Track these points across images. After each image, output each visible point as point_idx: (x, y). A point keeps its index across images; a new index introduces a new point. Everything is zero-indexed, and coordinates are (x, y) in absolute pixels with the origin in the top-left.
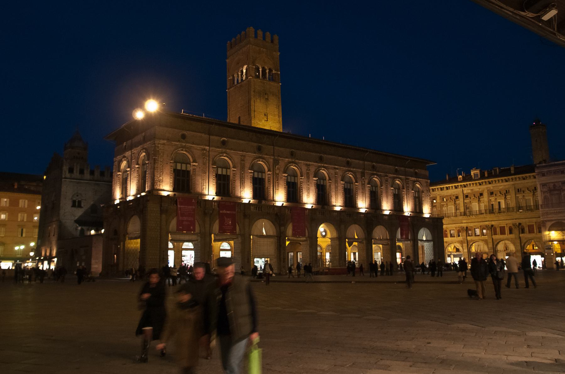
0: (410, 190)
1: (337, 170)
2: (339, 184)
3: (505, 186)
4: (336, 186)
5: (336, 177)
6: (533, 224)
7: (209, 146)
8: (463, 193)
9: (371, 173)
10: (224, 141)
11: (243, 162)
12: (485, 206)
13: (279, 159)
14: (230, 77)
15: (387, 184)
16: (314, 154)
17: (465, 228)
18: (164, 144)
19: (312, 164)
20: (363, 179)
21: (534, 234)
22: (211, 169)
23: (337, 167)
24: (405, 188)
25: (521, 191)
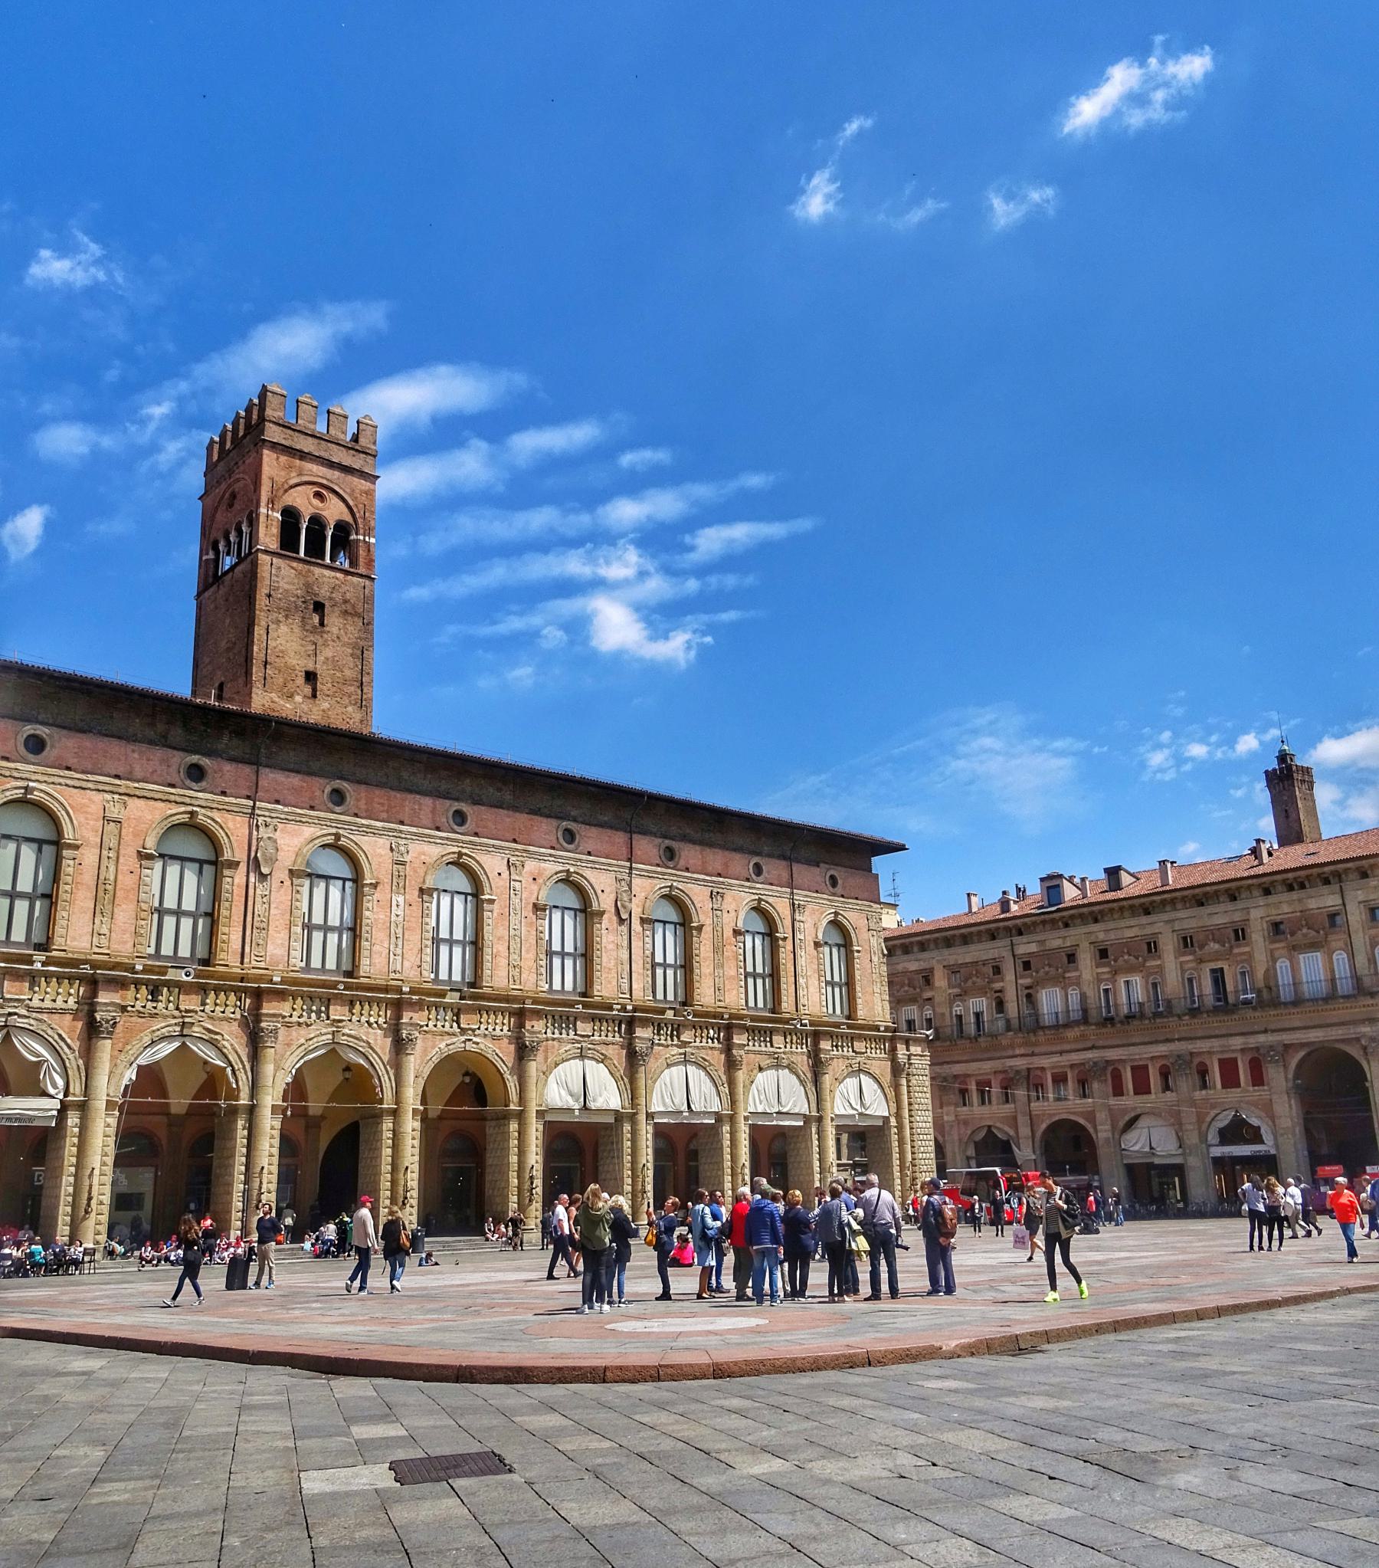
3: (1142, 926)
6: (1233, 1055)
8: (1014, 956)
12: (1083, 997)
14: (207, 554)
17: (1024, 1073)
21: (1239, 1090)
25: (1192, 946)
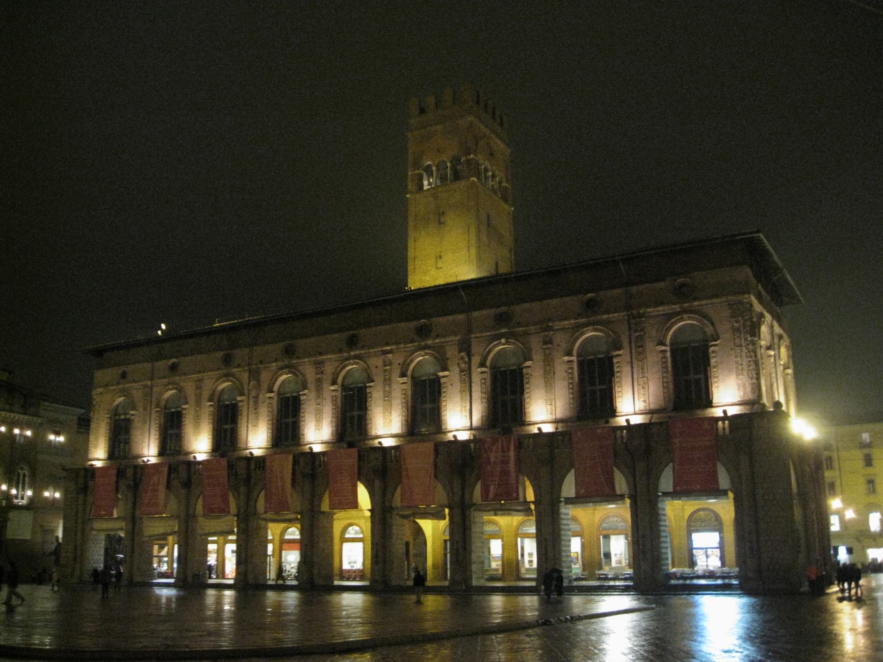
0: (650, 345)
1: (390, 356)
2: (394, 386)
4: (384, 392)
5: (385, 371)
7: (152, 379)
9: (491, 335)
10: (173, 364)
11: (198, 391)
13: (259, 368)
15: (547, 352)
16: (336, 335)
18: (101, 393)
19: (328, 359)
20: (462, 358)
22: (154, 415)
23: (389, 348)
24: (625, 343)
